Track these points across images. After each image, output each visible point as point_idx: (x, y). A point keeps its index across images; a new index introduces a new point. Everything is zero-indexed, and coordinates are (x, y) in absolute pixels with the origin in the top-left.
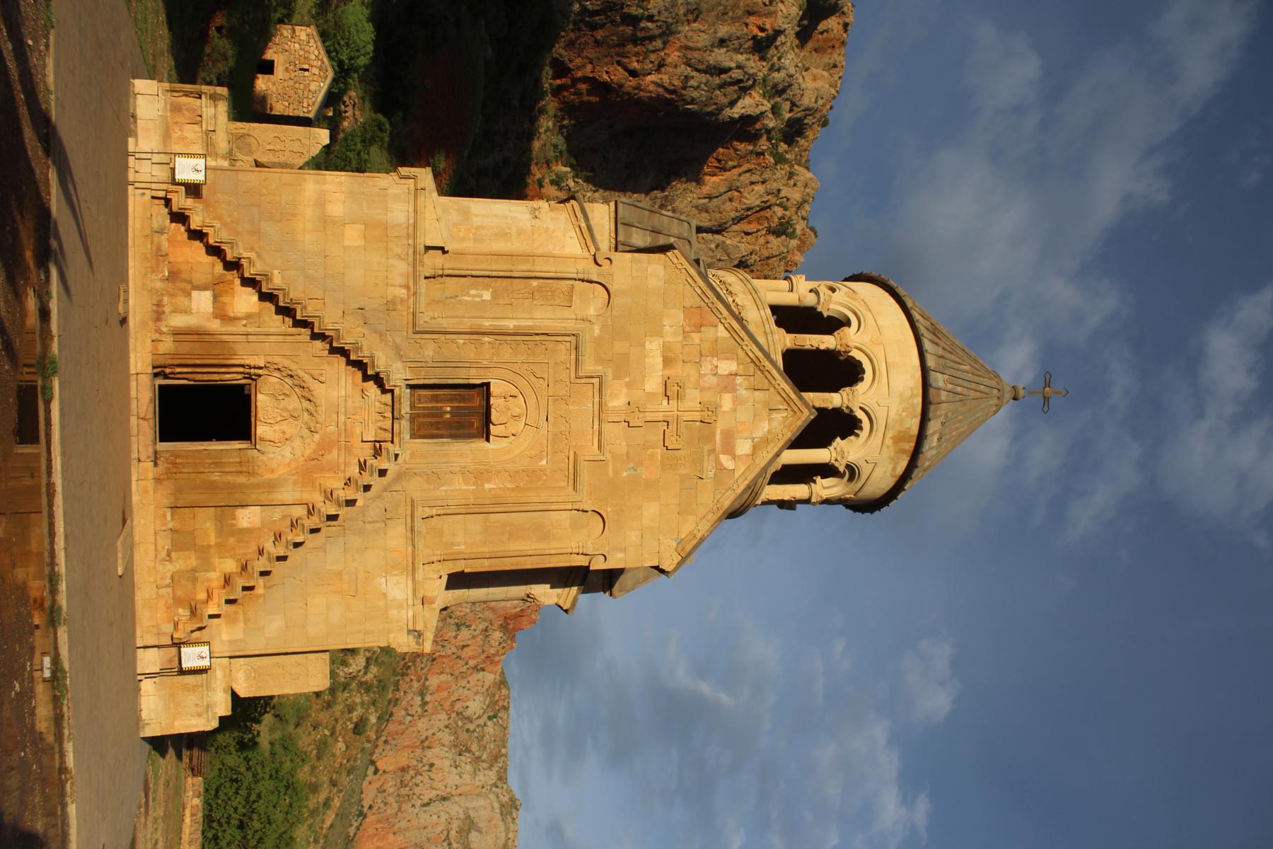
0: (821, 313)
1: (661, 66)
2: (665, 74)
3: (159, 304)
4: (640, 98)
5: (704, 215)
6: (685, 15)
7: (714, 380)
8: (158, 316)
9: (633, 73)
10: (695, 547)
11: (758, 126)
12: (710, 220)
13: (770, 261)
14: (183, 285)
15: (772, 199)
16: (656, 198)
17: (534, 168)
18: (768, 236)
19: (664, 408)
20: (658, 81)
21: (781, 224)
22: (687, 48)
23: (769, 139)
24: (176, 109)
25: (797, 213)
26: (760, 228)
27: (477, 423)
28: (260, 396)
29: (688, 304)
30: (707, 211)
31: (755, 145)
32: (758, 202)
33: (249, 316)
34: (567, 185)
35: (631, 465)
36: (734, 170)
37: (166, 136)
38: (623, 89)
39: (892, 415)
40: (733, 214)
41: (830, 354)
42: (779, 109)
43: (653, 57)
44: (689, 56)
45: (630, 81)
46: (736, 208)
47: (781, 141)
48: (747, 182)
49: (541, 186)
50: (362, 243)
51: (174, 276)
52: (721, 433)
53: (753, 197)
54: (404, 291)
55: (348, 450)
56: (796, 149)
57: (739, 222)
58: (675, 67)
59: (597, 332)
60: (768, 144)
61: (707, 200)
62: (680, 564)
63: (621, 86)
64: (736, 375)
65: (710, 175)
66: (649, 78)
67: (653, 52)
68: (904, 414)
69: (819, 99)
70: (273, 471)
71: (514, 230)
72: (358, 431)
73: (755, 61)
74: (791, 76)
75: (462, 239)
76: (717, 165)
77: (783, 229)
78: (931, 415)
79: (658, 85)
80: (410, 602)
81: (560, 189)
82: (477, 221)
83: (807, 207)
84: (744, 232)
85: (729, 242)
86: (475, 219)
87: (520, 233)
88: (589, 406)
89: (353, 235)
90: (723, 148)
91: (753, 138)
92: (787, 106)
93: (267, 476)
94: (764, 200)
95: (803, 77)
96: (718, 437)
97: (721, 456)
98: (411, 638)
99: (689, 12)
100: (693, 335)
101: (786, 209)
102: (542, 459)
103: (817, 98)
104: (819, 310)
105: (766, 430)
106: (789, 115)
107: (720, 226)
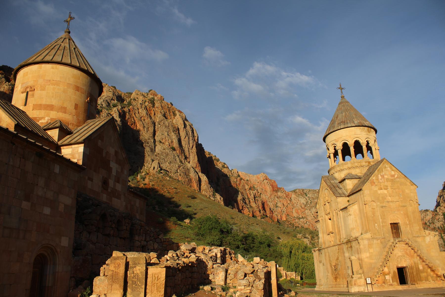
0: (342, 148)
3: (390, 285)
5: (150, 129)
7: (383, 179)
8: (392, 285)
10: (412, 182)
11: (121, 111)
12: (151, 127)
13: (163, 106)
14: (385, 281)
15: (143, 106)
16: (145, 145)
17: (140, 187)
18: (155, 107)
19: (389, 189)
21: (151, 103)
23: (124, 108)
24: (355, 284)
25: (147, 97)
26: (153, 110)
27: (395, 225)
28: (399, 266)
29: (370, 185)
30: (148, 128)
31: (127, 112)
32: (145, 111)
33: (388, 269)
34: (144, 175)
35: (400, 195)
36: (135, 119)
37: (360, 286)
39: (365, 134)
40: (149, 119)
41: (354, 147)
42: (114, 104)
46: (147, 118)
47: (123, 103)
48: (138, 115)
49: (146, 184)
50: (372, 249)
51: (384, 283)
52: (391, 177)
53: (143, 113)
54: (379, 240)
55: (407, 249)
56: (125, 97)
57: (151, 117)
59: (379, 203)
60: (126, 108)
61: (145, 128)
62: (415, 185)
64: (381, 175)
65: (137, 127)
68: (365, 131)
69: (110, 91)
70: (412, 263)
71: (355, 219)
72: (403, 248)
73: (103, 114)
74: (104, 100)
75: (358, 229)
76: (133, 125)
77: (152, 102)
78: (365, 125)
80: (429, 237)
81: (146, 177)
82: (355, 226)
83: (144, 94)
84: (154, 115)
85: (158, 120)
86: (354, 227)
87: (355, 218)
88: (391, 204)
89: (371, 250)
90: (128, 123)
91: (124, 113)
92: (113, 101)
93: (413, 264)
94: (144, 109)
95: (103, 96)
96: (392, 178)
97: (395, 177)
98: (435, 236)
100: (376, 184)
101: (146, 101)
102: (401, 213)
103: (109, 91)
104: (342, 149)
105: (389, 168)
106: (116, 101)
107: (153, 124)
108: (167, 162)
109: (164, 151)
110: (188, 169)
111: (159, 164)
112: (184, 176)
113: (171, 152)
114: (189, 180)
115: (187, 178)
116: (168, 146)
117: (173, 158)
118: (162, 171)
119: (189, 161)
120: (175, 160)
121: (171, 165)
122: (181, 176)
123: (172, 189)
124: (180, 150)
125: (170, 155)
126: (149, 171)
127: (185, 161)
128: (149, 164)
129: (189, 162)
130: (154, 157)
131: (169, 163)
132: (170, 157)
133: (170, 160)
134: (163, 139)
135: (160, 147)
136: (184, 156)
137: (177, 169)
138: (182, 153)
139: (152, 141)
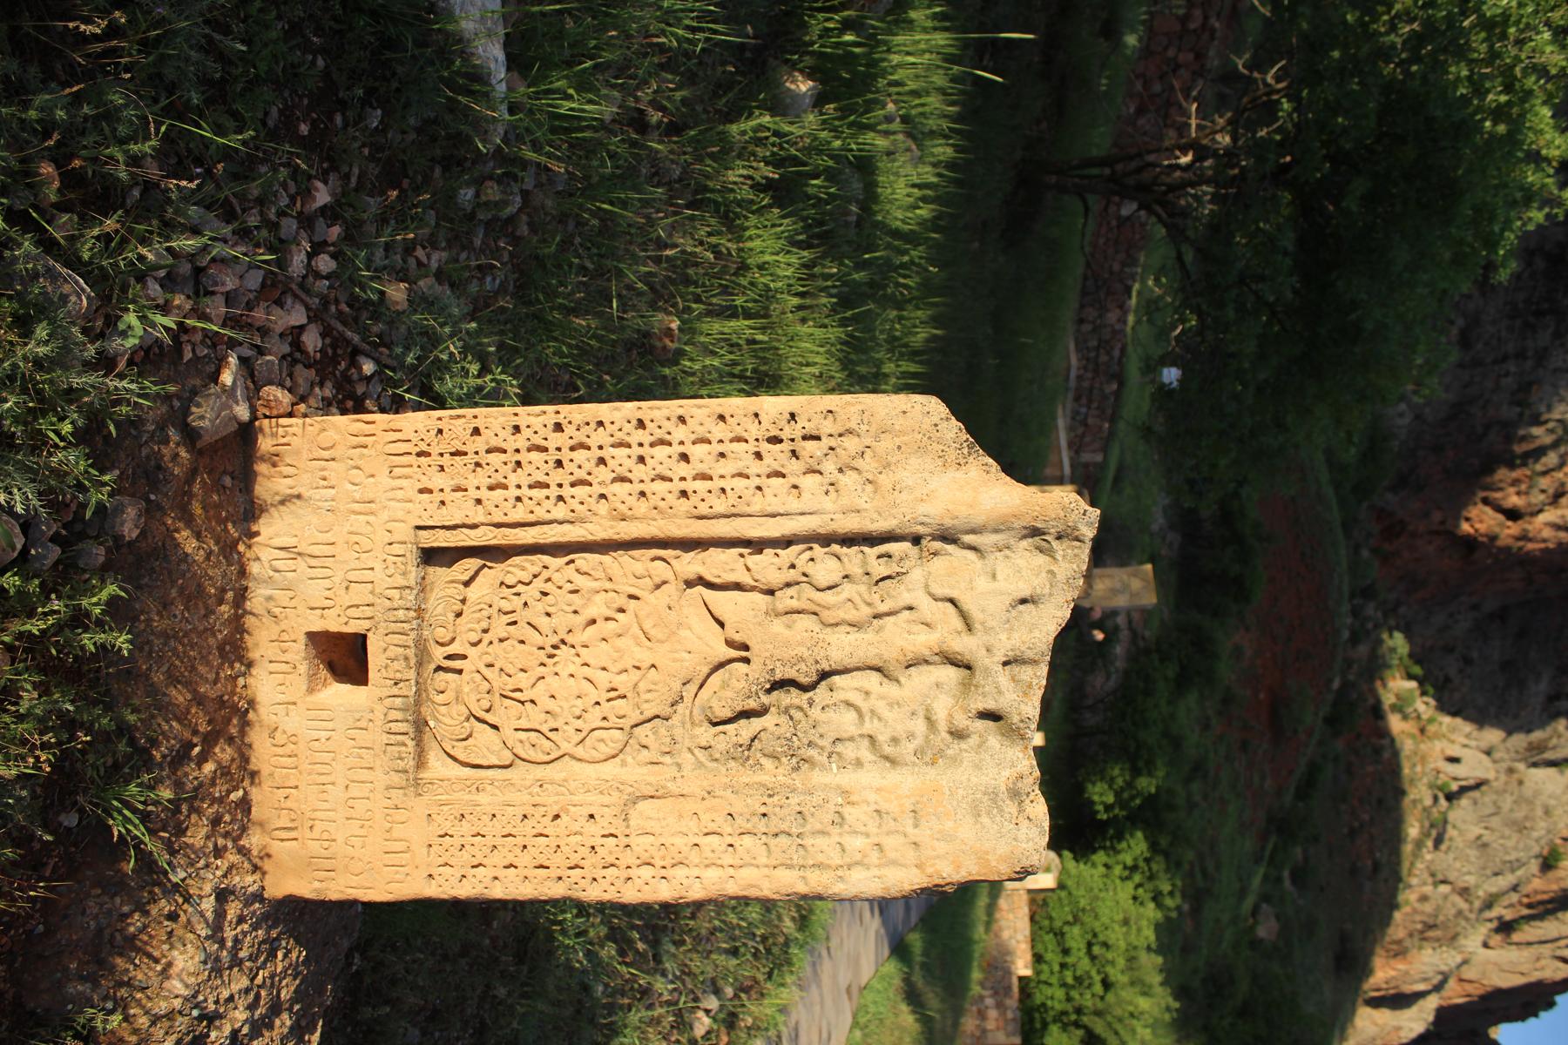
4: (1528, 553)
9: (1513, 515)
34: (1415, 710)
38: (1500, 543)
43: (1544, 482)
45: (1508, 527)
63: (1493, 538)
66: (1542, 518)
67: (1545, 473)
79: (1557, 527)
81: (1405, 717)
108: (1486, 828)
109: (1539, 812)
110: (1454, 937)
112: (1418, 918)
113: (1536, 849)
114: (1399, 942)
115: (1411, 935)
117: (1508, 858)
118: (1443, 802)
119: (1492, 943)
120: (1496, 870)
121: (1469, 851)
122: (1417, 905)
124: (1545, 897)
125: (1521, 845)
126: (1438, 736)
127: (1490, 920)
128: (1468, 736)
129: (1486, 945)
130: (1502, 760)
131: (1479, 837)
132: (1510, 843)
133: (1495, 845)
135: (1558, 791)
136: (1516, 916)
137: (1450, 883)
138: (1529, 906)
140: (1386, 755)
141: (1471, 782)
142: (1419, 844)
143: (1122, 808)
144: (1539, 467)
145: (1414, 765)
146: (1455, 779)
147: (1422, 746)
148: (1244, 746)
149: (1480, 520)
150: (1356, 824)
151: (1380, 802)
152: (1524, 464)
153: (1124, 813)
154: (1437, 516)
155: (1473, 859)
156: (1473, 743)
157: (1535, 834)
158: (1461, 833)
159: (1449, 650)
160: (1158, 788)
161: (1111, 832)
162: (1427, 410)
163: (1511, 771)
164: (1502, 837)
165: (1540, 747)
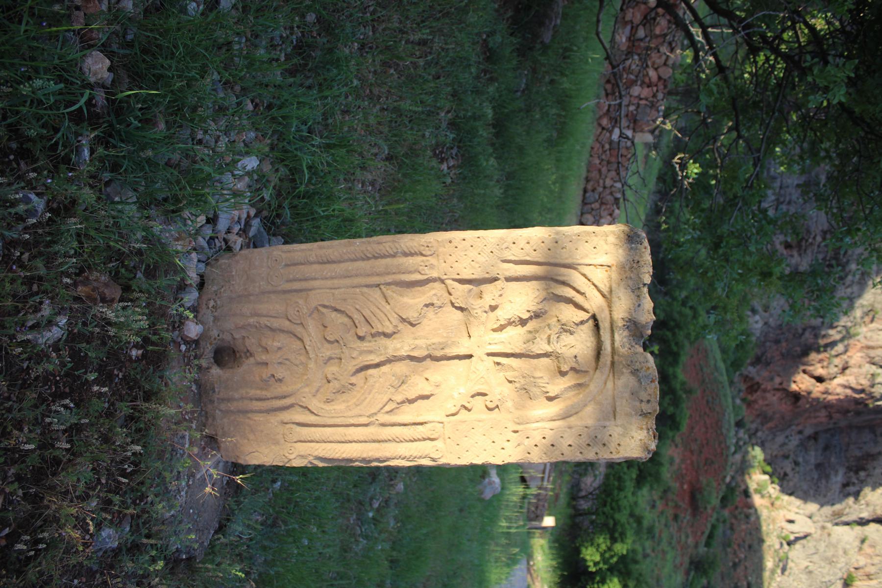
1: (845, 368)
2: (851, 375)
4: (829, 401)
6: (862, 318)
9: (820, 379)
20: (846, 383)
22: (869, 348)
38: (813, 396)
43: (836, 361)
44: (872, 355)
58: (860, 367)
63: (809, 393)
66: (836, 381)
67: (837, 356)
79: (845, 387)
81: (763, 496)
99: (867, 314)
109: (841, 552)
111: (805, 537)
113: (840, 575)
116: (856, 566)
117: (824, 580)
118: (786, 546)
121: (801, 575)
123: (746, 577)
125: (831, 572)
126: (782, 507)
128: (798, 507)
131: (807, 567)
132: (825, 571)
134: (872, 546)
139: (865, 515)
140: (753, 519)
141: (801, 535)
142: (773, 572)
143: (605, 563)
144: (833, 353)
145: (769, 525)
146: (792, 533)
147: (773, 513)
148: (676, 517)
149: (802, 383)
150: (737, 560)
151: (750, 547)
152: (825, 351)
153: (606, 567)
154: (777, 380)
155: (804, 580)
156: (801, 512)
157: (839, 566)
158: (797, 565)
159: (786, 457)
160: (628, 550)
161: (598, 578)
162: (771, 320)
163: (823, 528)
164: (820, 567)
165: (839, 514)
